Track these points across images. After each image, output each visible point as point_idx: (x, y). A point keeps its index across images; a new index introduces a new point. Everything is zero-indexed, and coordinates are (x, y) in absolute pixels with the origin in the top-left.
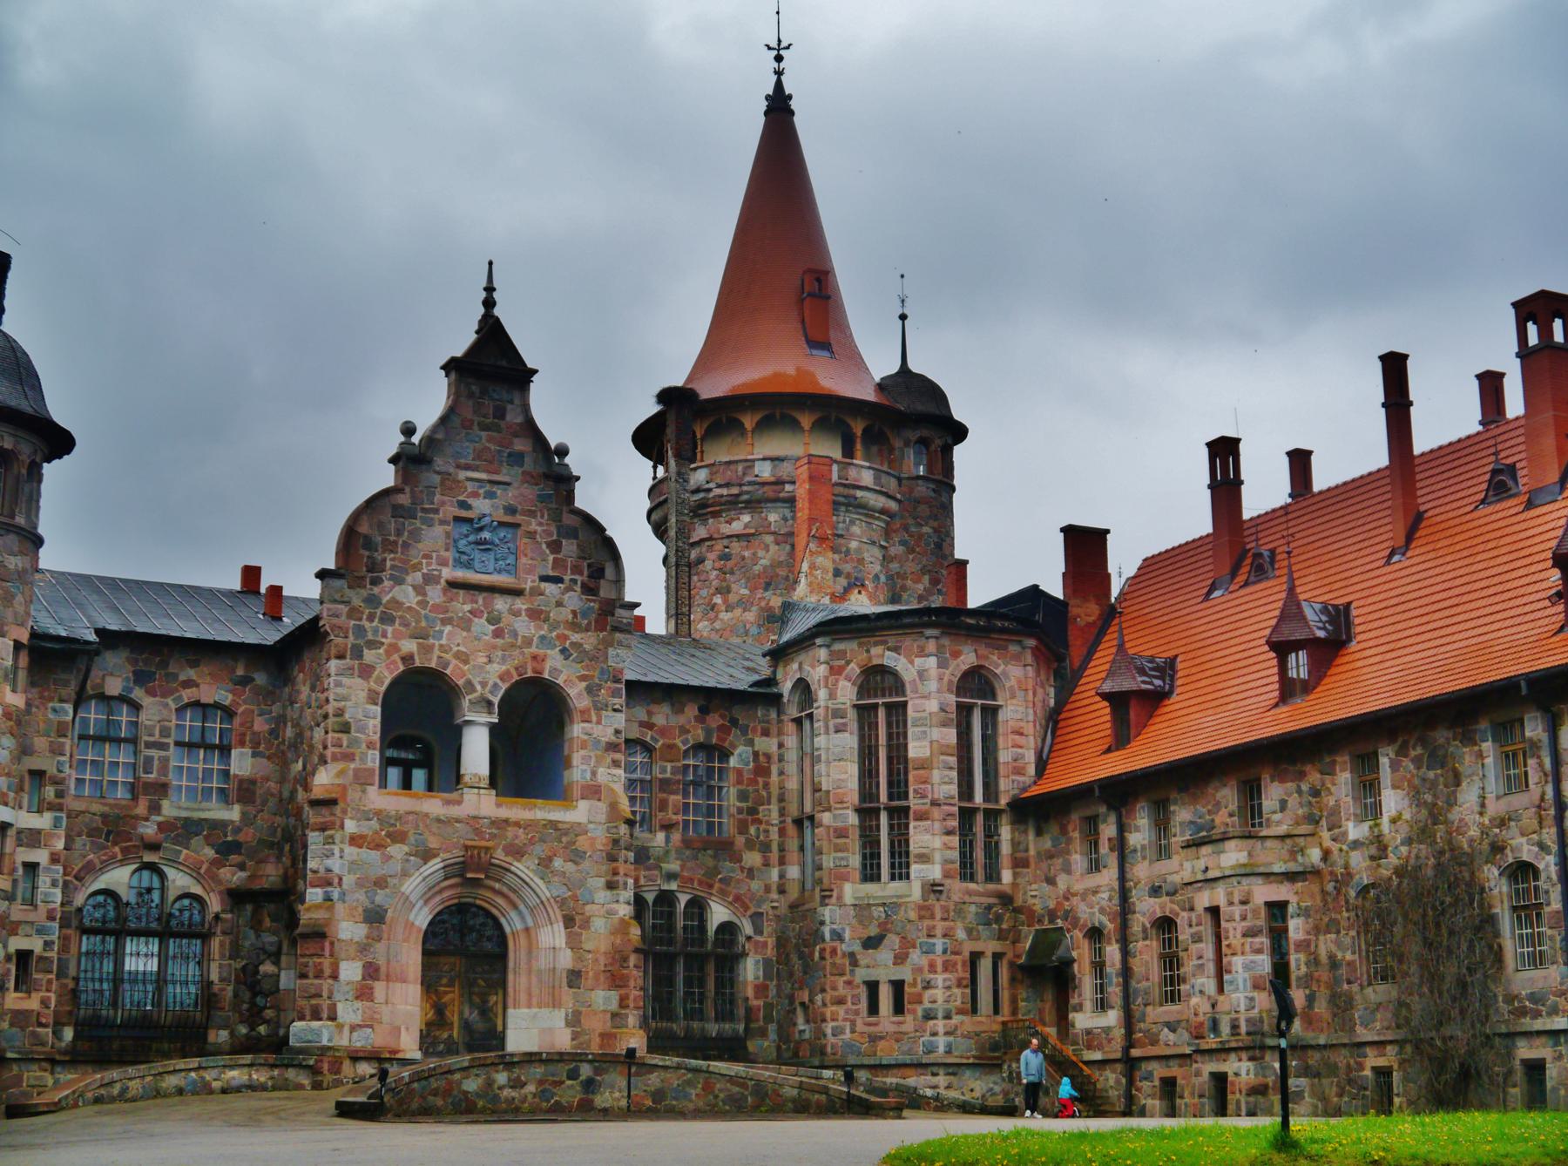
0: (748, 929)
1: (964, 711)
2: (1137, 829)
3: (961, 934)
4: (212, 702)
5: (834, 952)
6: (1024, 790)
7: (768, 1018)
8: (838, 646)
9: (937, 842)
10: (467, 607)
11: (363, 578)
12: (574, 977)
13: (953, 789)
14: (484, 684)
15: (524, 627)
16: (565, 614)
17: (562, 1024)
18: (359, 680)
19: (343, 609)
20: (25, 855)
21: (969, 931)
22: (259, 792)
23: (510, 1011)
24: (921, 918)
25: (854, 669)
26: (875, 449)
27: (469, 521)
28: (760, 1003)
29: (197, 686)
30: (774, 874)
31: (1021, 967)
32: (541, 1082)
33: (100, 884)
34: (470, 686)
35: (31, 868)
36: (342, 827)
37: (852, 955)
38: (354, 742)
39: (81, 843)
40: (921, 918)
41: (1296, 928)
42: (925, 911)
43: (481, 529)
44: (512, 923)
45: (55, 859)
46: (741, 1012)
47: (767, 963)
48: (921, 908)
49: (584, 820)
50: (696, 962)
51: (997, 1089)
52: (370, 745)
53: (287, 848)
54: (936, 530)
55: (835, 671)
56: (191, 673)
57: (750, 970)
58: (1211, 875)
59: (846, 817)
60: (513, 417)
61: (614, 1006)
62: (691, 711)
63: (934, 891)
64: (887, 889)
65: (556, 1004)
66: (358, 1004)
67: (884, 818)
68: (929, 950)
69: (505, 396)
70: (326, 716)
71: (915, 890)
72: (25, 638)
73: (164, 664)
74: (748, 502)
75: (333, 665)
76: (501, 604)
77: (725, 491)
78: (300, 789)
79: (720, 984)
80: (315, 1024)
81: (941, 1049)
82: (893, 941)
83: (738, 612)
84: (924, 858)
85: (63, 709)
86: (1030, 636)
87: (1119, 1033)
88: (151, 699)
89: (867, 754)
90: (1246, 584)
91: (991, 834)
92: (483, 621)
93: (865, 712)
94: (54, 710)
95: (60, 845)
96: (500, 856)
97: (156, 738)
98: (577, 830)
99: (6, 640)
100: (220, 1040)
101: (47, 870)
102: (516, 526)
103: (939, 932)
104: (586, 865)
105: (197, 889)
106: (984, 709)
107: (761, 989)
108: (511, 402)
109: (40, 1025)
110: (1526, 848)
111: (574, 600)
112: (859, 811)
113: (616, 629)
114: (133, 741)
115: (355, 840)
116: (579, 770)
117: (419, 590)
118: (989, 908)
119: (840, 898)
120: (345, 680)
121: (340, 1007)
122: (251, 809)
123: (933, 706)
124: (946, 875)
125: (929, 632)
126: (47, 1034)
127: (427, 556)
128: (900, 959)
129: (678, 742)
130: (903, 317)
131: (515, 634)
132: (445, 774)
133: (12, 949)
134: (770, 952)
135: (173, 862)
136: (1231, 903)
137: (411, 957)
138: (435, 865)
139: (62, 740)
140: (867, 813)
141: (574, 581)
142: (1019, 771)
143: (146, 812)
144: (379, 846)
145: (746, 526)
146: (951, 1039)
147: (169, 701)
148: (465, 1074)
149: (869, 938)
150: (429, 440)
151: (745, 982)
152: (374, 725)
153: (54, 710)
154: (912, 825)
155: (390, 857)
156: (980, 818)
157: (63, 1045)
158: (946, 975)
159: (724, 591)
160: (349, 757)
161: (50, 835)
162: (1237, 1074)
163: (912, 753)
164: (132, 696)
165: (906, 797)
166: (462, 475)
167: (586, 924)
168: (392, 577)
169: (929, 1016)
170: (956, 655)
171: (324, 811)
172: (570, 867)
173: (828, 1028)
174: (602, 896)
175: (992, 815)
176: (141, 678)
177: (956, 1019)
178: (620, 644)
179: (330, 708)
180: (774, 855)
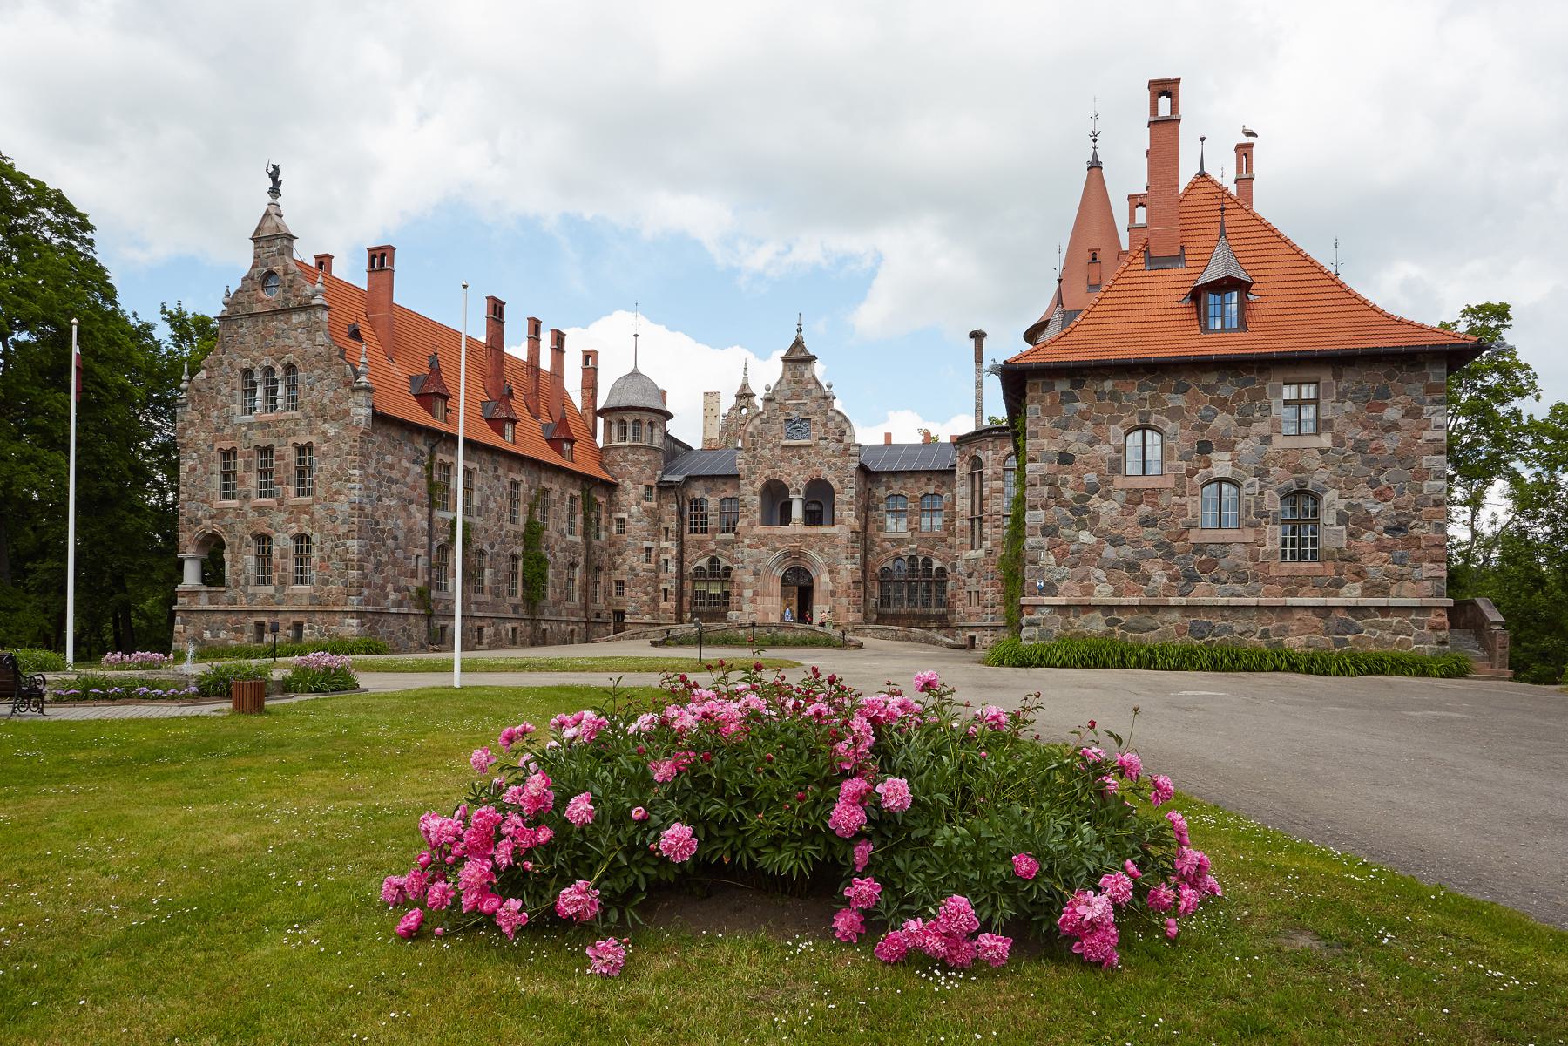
8: (963, 449)
12: (833, 594)
15: (813, 459)
16: (830, 451)
20: (663, 556)
35: (666, 561)
37: (964, 581)
44: (814, 574)
52: (754, 511)
55: (962, 459)
60: (807, 375)
62: (924, 480)
71: (980, 553)
72: (653, 483)
76: (803, 451)
82: (976, 574)
84: (986, 540)
93: (972, 475)
95: (675, 552)
96: (803, 549)
98: (834, 536)
105: (730, 565)
111: (834, 445)
112: (970, 519)
115: (749, 546)
117: (771, 450)
121: (744, 606)
123: (990, 472)
125: (989, 439)
128: (978, 582)
131: (809, 462)
132: (786, 519)
135: (721, 555)
137: (776, 587)
138: (779, 553)
140: (972, 520)
150: (774, 391)
155: (761, 552)
160: (747, 516)
166: (787, 402)
167: (838, 573)
170: (1002, 448)
174: (845, 561)
176: (708, 491)
178: (853, 461)
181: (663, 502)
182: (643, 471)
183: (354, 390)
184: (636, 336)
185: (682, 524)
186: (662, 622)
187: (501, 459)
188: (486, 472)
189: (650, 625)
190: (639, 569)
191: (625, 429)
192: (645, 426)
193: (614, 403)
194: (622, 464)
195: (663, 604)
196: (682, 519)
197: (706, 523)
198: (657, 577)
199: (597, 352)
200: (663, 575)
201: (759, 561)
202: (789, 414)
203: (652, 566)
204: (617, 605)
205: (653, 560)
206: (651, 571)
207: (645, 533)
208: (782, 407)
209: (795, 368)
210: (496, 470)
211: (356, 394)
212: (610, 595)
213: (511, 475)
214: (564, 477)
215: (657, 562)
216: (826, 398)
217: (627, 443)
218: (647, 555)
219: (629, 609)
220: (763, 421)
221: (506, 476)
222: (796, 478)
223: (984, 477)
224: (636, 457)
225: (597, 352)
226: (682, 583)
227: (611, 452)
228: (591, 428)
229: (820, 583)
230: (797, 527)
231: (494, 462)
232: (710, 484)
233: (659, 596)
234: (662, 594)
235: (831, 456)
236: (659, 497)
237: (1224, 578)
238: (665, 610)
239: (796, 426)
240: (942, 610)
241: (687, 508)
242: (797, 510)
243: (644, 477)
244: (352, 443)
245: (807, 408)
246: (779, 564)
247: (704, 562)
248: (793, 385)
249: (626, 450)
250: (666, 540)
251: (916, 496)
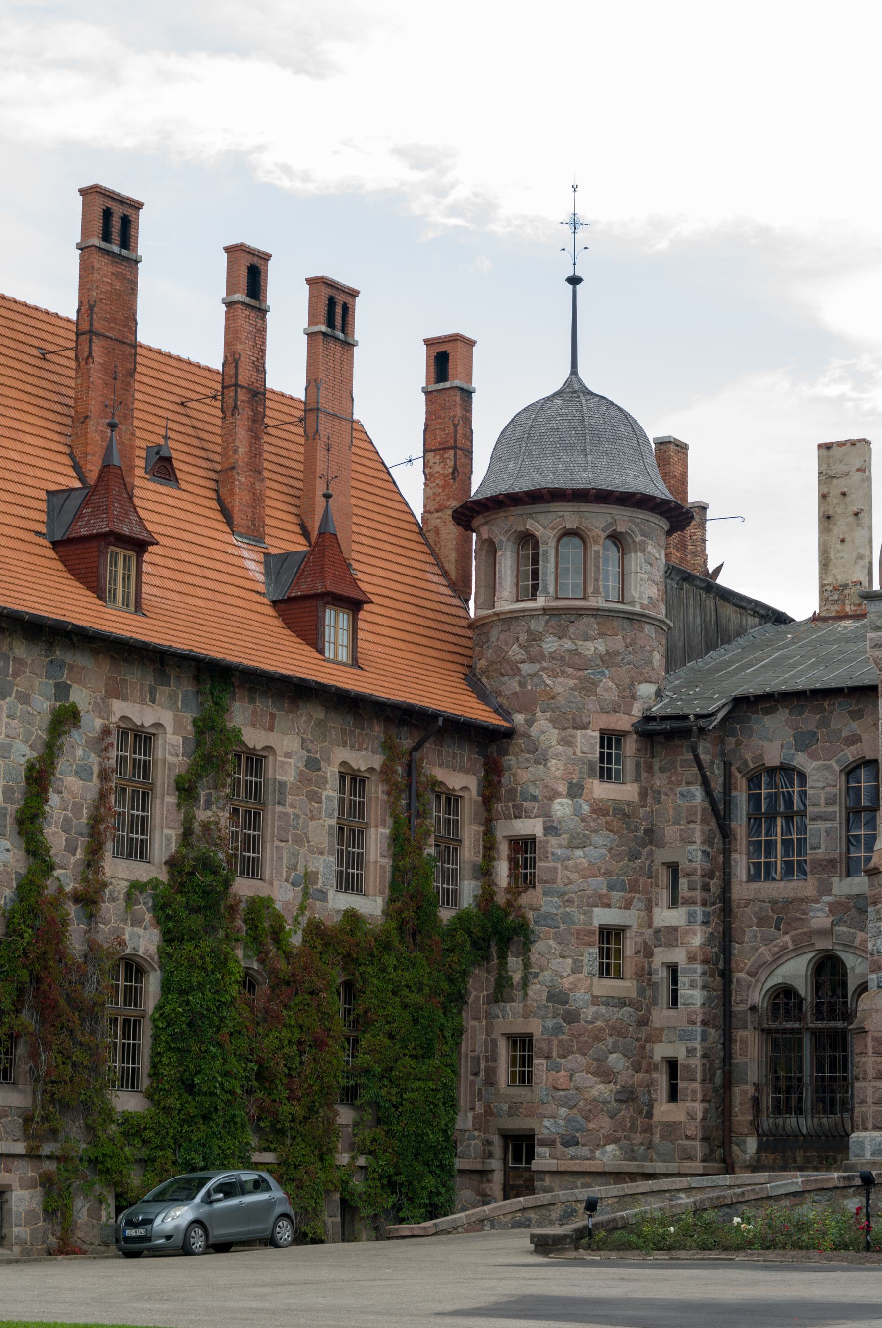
33: (777, 979)
39: (751, 935)
45: (692, 959)
56: (854, 726)
72: (623, 722)
73: (824, 723)
85: (689, 792)
88: (815, 764)
94: (682, 795)
95: (697, 940)
97: (822, 809)
99: (589, 732)
101: (686, 971)
109: (687, 1138)
114: (802, 814)
126: (694, 1147)
133: (657, 1058)
139: (691, 826)
143: (815, 893)
147: (833, 763)
148: (797, 1200)
153: (682, 795)
157: (748, 1157)
161: (687, 932)
164: (795, 763)
176: (805, 742)
181: (659, 780)
182: (588, 687)
184: (574, 281)
185: (727, 852)
186: (660, 1167)
187: (81, 660)
188: (24, 699)
189: (618, 1176)
190: (579, 997)
191: (535, 560)
192: (600, 548)
193: (502, 487)
194: (526, 668)
195: (664, 1111)
196: (726, 833)
197: (802, 842)
198: (643, 1022)
199: (471, 343)
200: (661, 1016)
203: (625, 987)
204: (510, 1115)
205: (629, 967)
206: (622, 1002)
207: (599, 883)
210: (62, 690)
212: (491, 1081)
213: (119, 708)
214: (319, 713)
215: (644, 975)
217: (540, 602)
218: (605, 953)
219: (546, 1128)
221: (103, 710)
224: (568, 644)
225: (471, 343)
226: (727, 1041)
227: (494, 634)
228: (451, 568)
231: (55, 666)
232: (810, 720)
233: (650, 1085)
234: (662, 1079)
236: (644, 769)
238: (671, 1129)
241: (741, 797)
243: (592, 704)
249: (537, 625)
250: (674, 903)
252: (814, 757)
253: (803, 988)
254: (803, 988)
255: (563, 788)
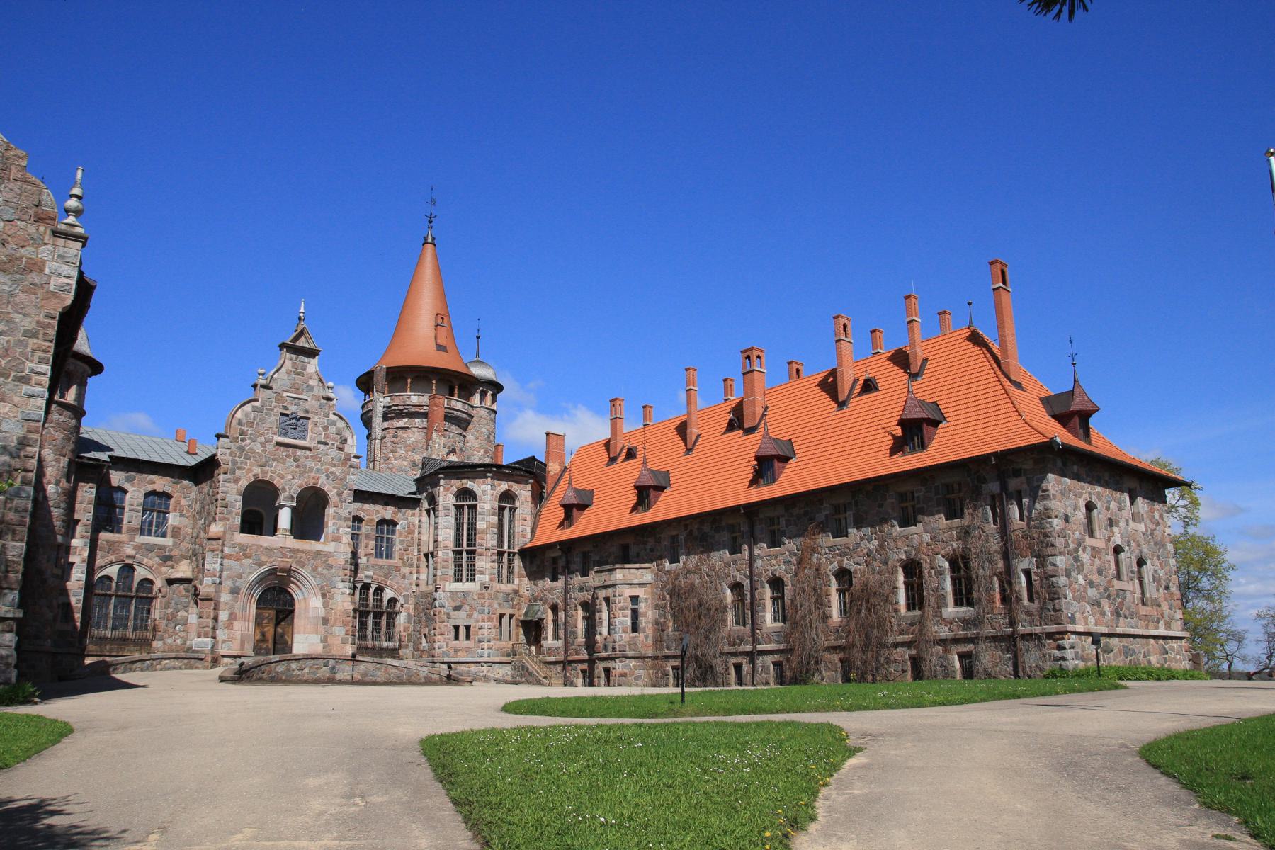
0: (401, 601)
1: (501, 509)
2: (574, 563)
3: (496, 606)
4: (161, 490)
5: (440, 612)
6: (526, 544)
7: (409, 640)
9: (488, 565)
10: (284, 454)
11: (237, 438)
12: (325, 621)
13: (495, 543)
14: (290, 489)
15: (310, 463)
17: (319, 641)
18: (233, 485)
19: (228, 451)
21: (500, 604)
22: (182, 533)
23: (296, 636)
24: (479, 598)
25: (454, 489)
26: (463, 393)
27: (287, 415)
28: (405, 634)
29: (154, 483)
30: (415, 577)
31: (521, 621)
32: (311, 667)
34: (284, 490)
36: (222, 551)
37: (448, 614)
38: (230, 512)
40: (479, 598)
41: (642, 607)
42: (481, 596)
43: (293, 419)
46: (397, 638)
47: (409, 616)
48: (479, 594)
49: (333, 551)
50: (378, 615)
51: (509, 673)
53: (194, 559)
54: (488, 430)
57: (401, 620)
58: (608, 583)
59: (448, 554)
61: (343, 633)
63: (485, 587)
64: (465, 586)
65: (317, 633)
66: (226, 631)
67: (465, 553)
68: (483, 612)
69: (306, 359)
70: (217, 500)
74: (406, 413)
75: (222, 477)
76: (299, 452)
77: (396, 408)
78: (202, 533)
79: (388, 624)
80: (205, 640)
81: (486, 655)
83: (400, 461)
84: (482, 572)
86: (531, 478)
87: (562, 650)
89: (459, 526)
90: (624, 460)
91: (510, 562)
92: (291, 460)
95: (86, 554)
98: (328, 555)
100: (159, 646)
101: (78, 566)
102: (308, 419)
103: (487, 605)
104: (333, 571)
106: (510, 509)
107: (406, 629)
108: (309, 363)
110: (738, 576)
111: (333, 452)
113: (351, 467)
115: (229, 557)
116: (330, 526)
117: (263, 445)
118: (509, 594)
119: (443, 589)
120: (228, 484)
122: (178, 541)
123: (488, 506)
124: (491, 580)
125: (489, 474)
127: (267, 430)
128: (469, 616)
129: (375, 517)
130: (478, 338)
131: (305, 466)
134: (411, 612)
135: (140, 564)
136: (614, 596)
138: (264, 569)
140: (458, 553)
141: (333, 444)
142: (524, 536)
144: (237, 560)
145: (405, 424)
146: (490, 651)
149: (456, 607)
151: (400, 624)
152: (239, 504)
154: (477, 557)
155: (242, 565)
156: (506, 555)
158: (489, 623)
159: (393, 451)
162: (614, 669)
163: (478, 527)
165: (475, 546)
166: (285, 394)
167: (331, 598)
168: (251, 438)
169: (481, 642)
170: (499, 485)
171: (214, 542)
172: (325, 571)
173: (436, 646)
174: (340, 585)
175: (511, 554)
176: (128, 480)
177: (491, 643)
179: (219, 497)
180: (415, 570)
183: (57, 234)
201: (240, 576)
202: (285, 408)
208: (279, 398)
209: (296, 358)
211: (61, 241)
216: (329, 399)
220: (255, 410)
222: (290, 483)
223: (478, 508)
224: (62, 418)
229: (306, 609)
230: (283, 539)
235: (329, 464)
237: (1127, 613)
239: (294, 422)
240: (391, 644)
242: (285, 519)
244: (41, 318)
245: (307, 405)
246: (261, 580)
247: (113, 571)
248: (292, 376)
251: (372, 520)
252: (133, 485)
253: (115, 577)
254: (115, 577)
255: (54, 481)
